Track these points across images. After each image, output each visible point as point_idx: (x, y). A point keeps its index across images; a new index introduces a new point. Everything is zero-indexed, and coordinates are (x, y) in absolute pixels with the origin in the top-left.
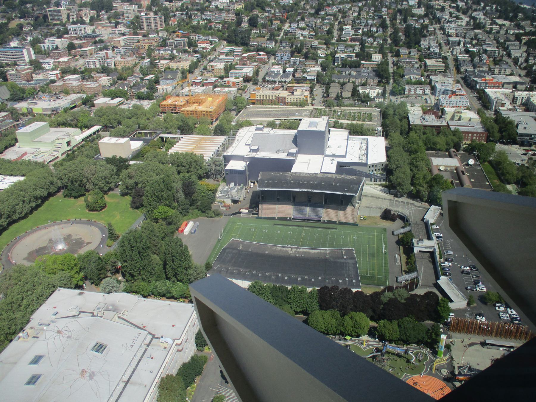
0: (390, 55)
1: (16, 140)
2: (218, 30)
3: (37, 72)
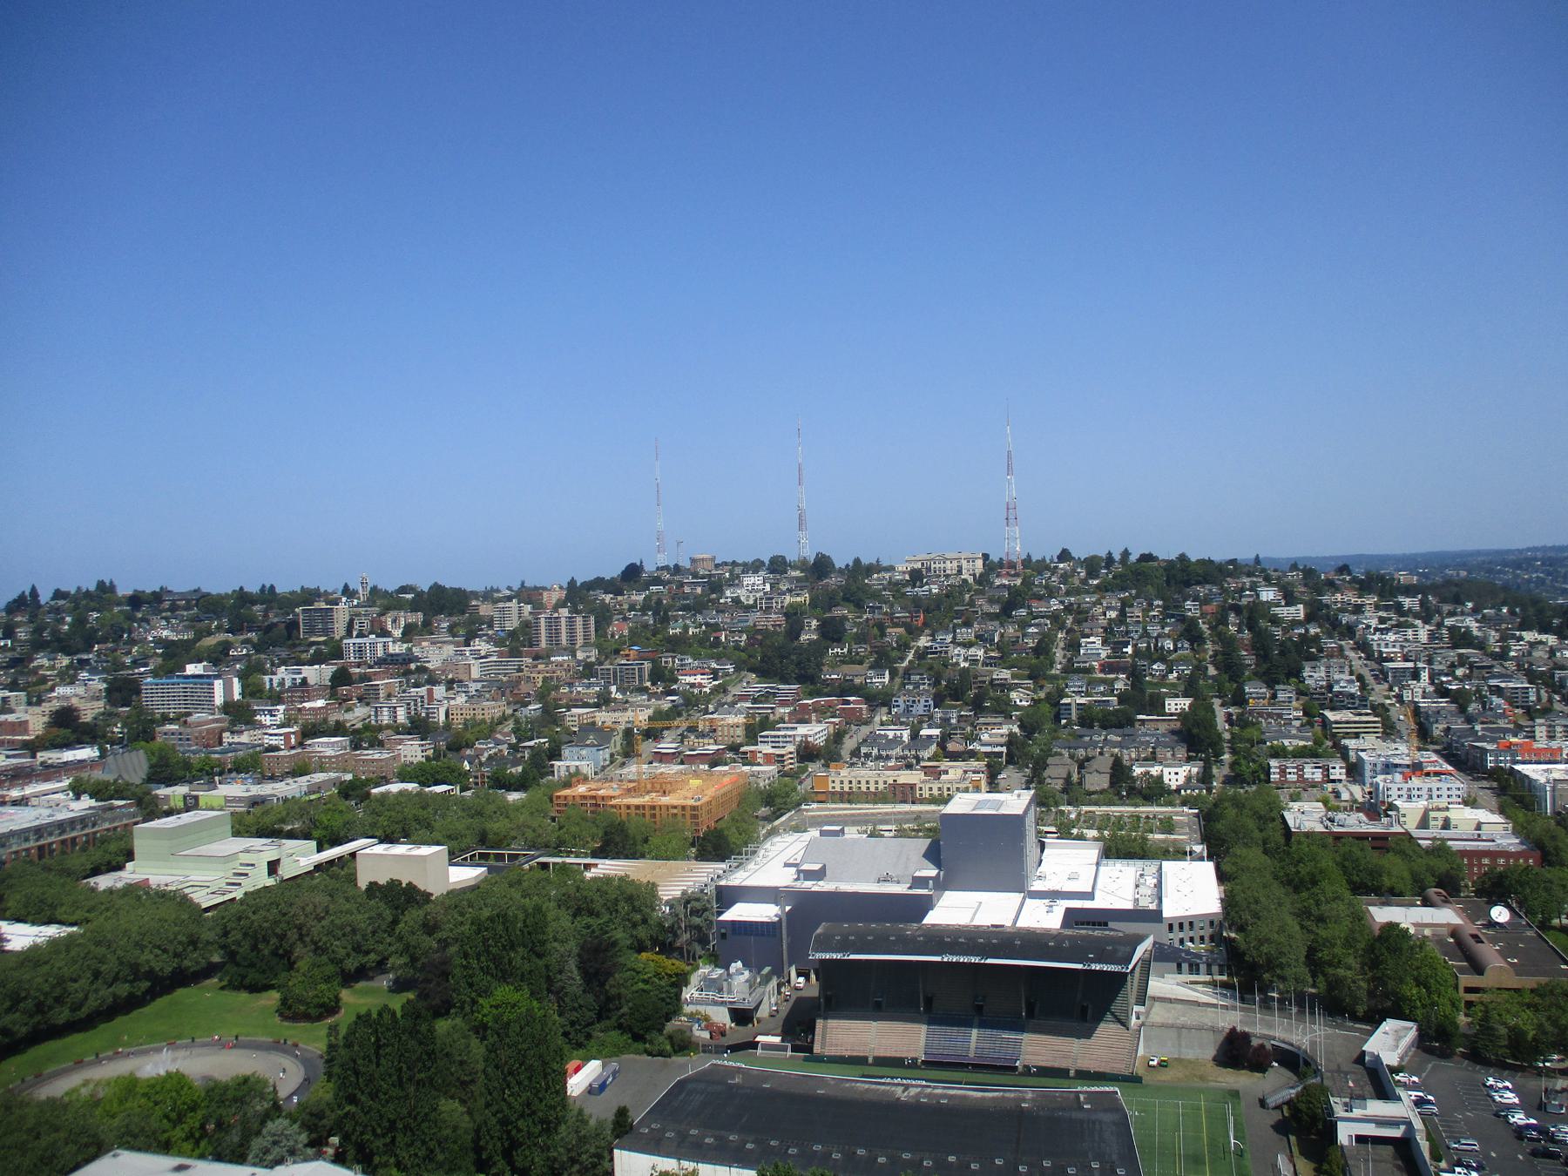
0: (1217, 702)
2: (737, 647)
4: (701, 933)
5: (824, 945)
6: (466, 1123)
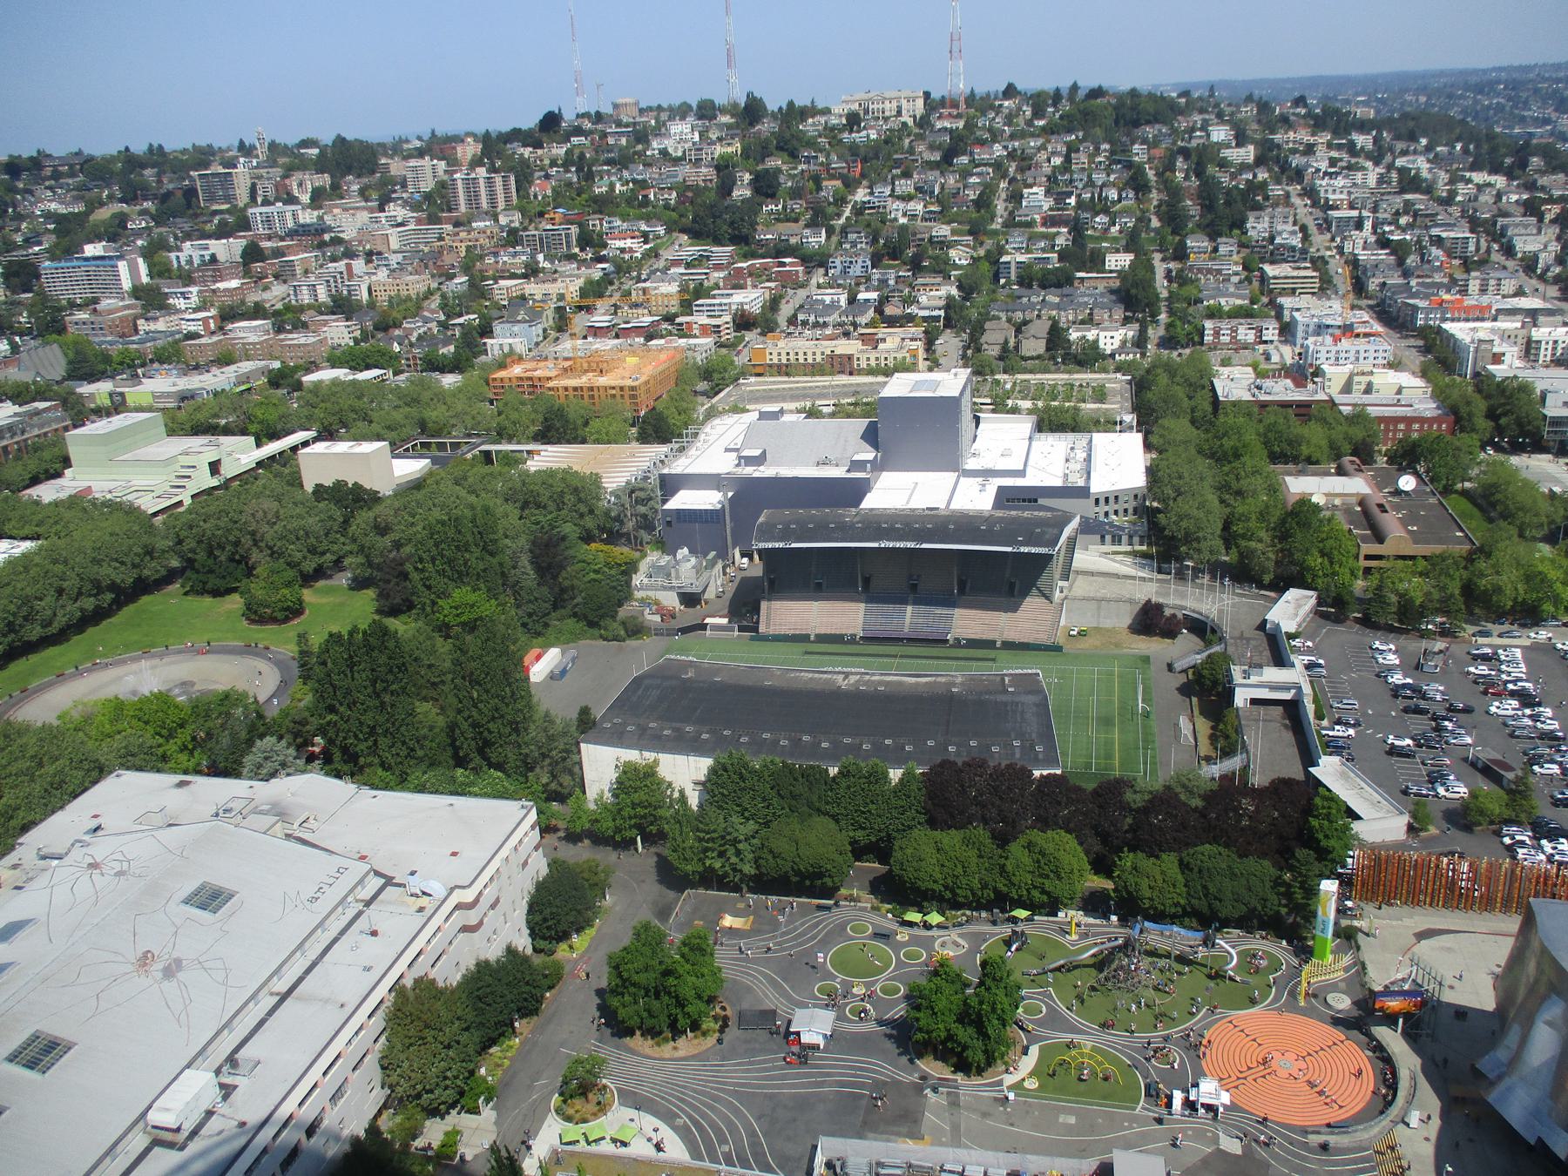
0: (1157, 257)
2: (667, 207)
4: (647, 520)
5: (767, 532)
6: (441, 721)
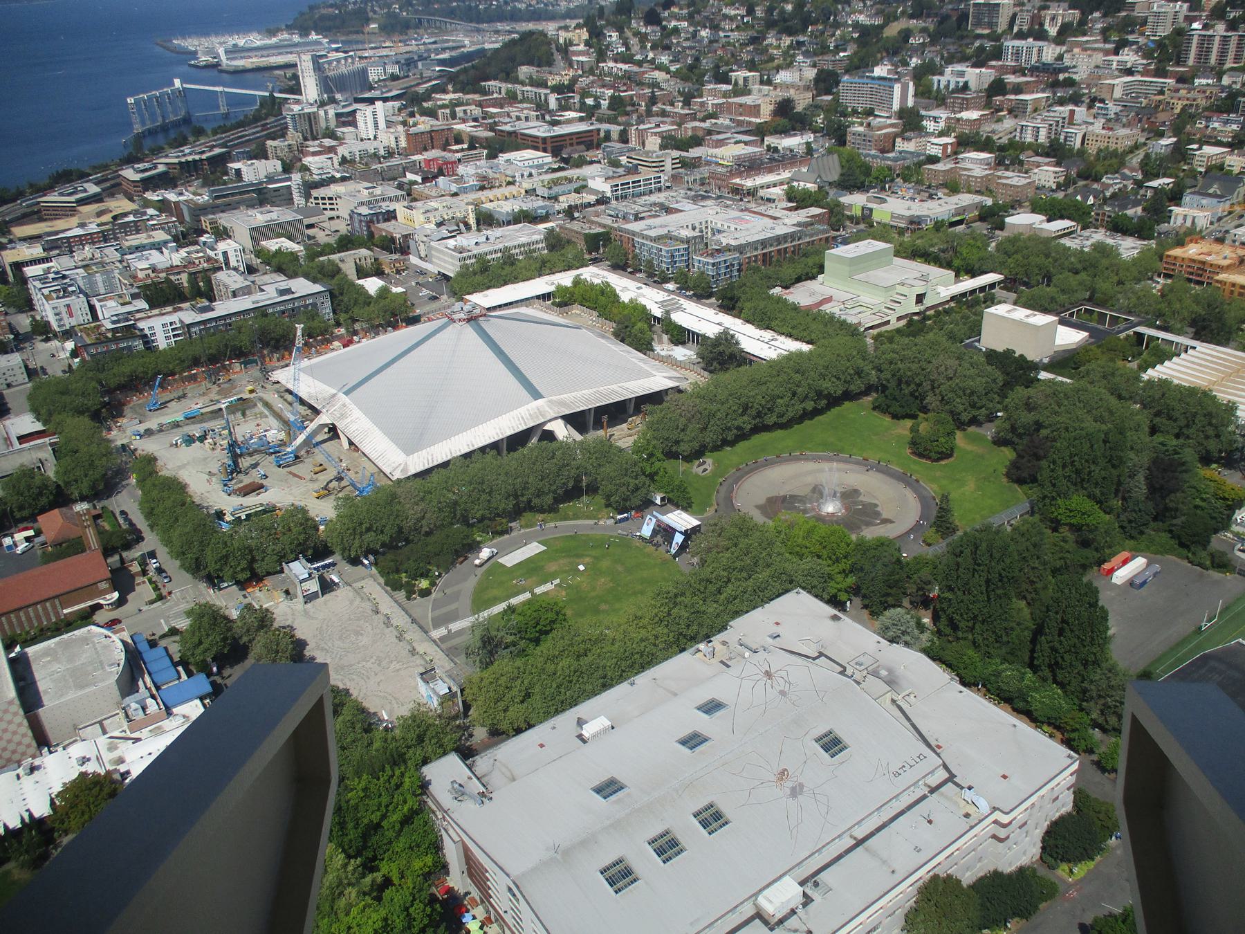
1: (821, 269)
3: (907, 134)
